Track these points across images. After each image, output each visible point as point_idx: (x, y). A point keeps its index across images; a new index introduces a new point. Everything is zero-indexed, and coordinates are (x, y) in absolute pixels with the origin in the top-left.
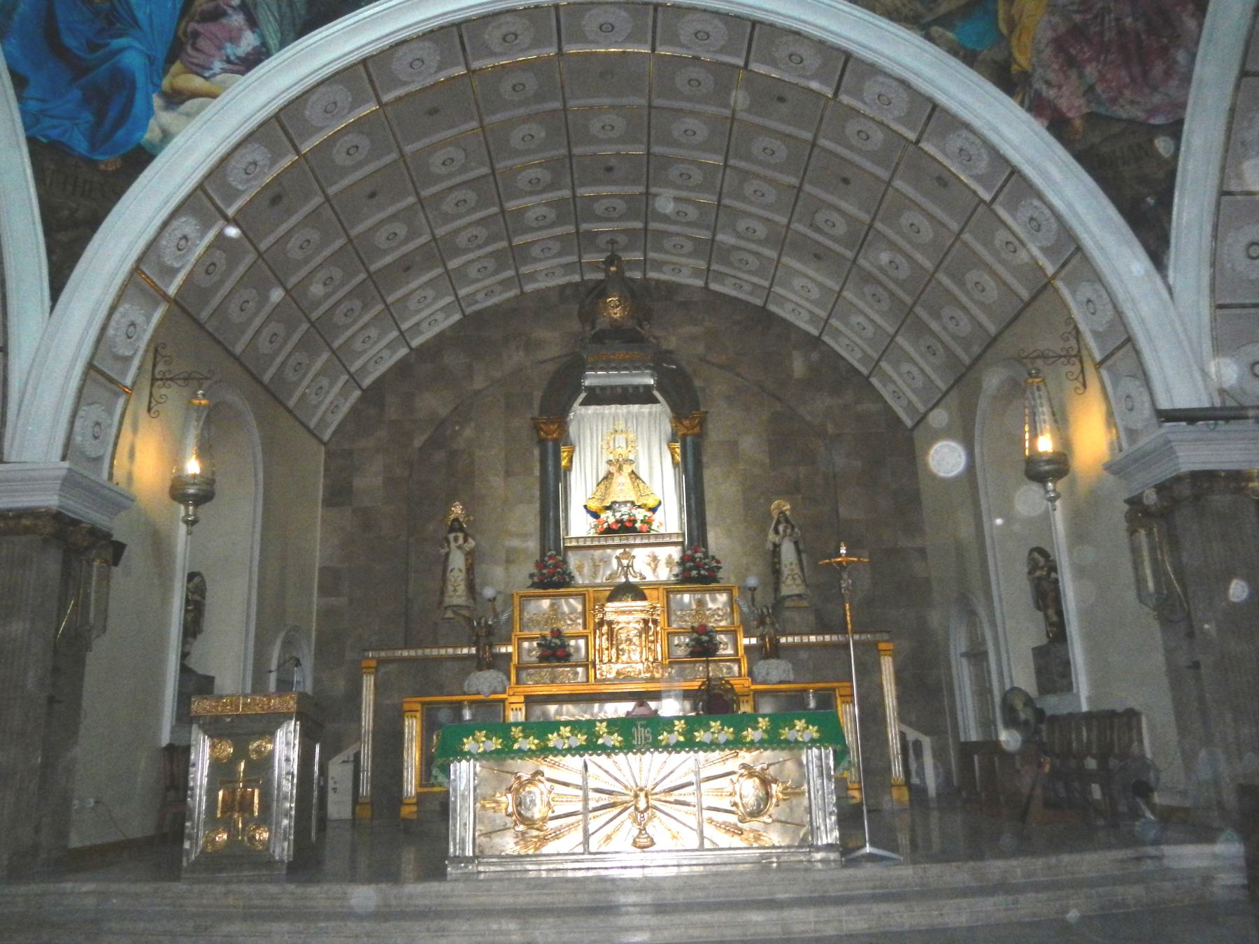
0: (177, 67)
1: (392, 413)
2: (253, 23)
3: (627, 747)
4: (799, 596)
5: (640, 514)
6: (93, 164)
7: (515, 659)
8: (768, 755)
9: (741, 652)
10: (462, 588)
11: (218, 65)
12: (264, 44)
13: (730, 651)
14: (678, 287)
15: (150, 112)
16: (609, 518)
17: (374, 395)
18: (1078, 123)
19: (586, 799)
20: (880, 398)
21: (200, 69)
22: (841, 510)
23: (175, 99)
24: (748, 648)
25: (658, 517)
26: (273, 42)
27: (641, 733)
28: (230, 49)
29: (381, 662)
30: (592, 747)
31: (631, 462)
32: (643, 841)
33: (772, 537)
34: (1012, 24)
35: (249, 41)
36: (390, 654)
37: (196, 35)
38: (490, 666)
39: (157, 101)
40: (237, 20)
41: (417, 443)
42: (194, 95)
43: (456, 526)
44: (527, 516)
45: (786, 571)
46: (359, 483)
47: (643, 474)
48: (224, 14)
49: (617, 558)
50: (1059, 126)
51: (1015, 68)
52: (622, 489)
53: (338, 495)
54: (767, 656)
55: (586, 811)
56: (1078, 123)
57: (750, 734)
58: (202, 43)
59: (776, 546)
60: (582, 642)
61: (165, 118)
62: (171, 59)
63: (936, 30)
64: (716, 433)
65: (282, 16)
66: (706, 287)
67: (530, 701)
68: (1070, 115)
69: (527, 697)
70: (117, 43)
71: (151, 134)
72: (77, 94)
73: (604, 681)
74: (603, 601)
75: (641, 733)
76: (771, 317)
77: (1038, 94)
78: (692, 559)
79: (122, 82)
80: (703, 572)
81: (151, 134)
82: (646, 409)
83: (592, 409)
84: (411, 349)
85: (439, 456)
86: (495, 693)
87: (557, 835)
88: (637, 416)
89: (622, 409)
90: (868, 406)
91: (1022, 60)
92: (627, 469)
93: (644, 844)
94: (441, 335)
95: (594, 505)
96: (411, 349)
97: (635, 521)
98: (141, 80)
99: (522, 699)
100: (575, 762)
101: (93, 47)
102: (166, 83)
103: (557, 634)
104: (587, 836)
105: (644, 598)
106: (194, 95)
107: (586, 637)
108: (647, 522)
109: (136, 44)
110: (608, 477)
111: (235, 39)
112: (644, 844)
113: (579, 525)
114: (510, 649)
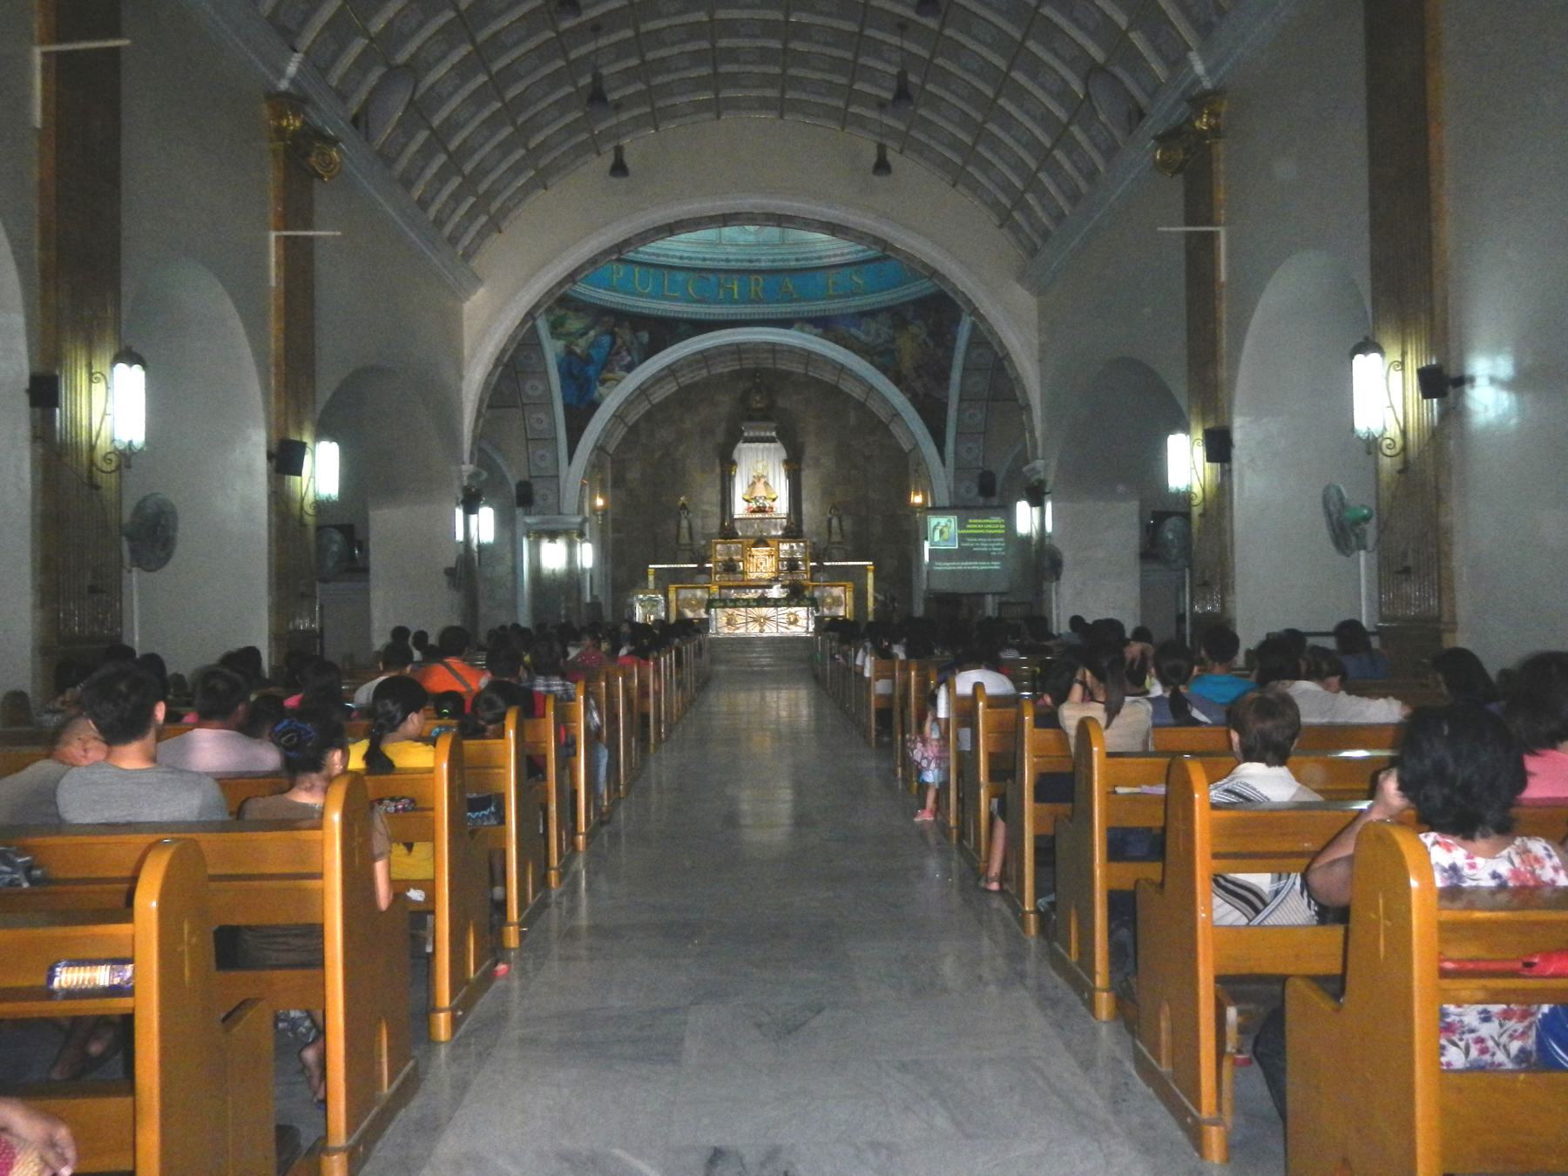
0: (604, 371)
2: (629, 353)
3: (758, 606)
4: (839, 543)
5: (768, 503)
8: (797, 609)
10: (687, 536)
11: (617, 369)
12: (633, 360)
13: (803, 568)
14: (792, 373)
15: (596, 387)
16: (753, 505)
17: (633, 430)
20: (891, 436)
21: (612, 371)
23: (603, 382)
25: (776, 504)
26: (636, 360)
27: (762, 602)
29: (656, 569)
30: (748, 606)
31: (763, 476)
33: (829, 516)
35: (629, 358)
39: (598, 384)
40: (624, 353)
41: (658, 454)
42: (610, 379)
43: (684, 506)
44: (712, 495)
45: (833, 531)
46: (630, 476)
47: (771, 483)
50: (915, 401)
52: (760, 491)
53: (618, 482)
57: (792, 603)
59: (830, 521)
61: (601, 389)
62: (603, 369)
63: (875, 358)
64: (810, 451)
66: (806, 375)
67: (721, 588)
71: (596, 395)
73: (751, 580)
75: (762, 602)
76: (841, 392)
82: (773, 445)
83: (746, 445)
87: (738, 628)
88: (769, 450)
89: (761, 445)
92: (763, 480)
93: (762, 631)
95: (747, 497)
100: (743, 609)
102: (601, 377)
103: (731, 560)
105: (768, 546)
106: (610, 379)
108: (771, 508)
110: (754, 483)
111: (623, 360)
112: (762, 631)
113: (740, 509)
114: (711, 565)
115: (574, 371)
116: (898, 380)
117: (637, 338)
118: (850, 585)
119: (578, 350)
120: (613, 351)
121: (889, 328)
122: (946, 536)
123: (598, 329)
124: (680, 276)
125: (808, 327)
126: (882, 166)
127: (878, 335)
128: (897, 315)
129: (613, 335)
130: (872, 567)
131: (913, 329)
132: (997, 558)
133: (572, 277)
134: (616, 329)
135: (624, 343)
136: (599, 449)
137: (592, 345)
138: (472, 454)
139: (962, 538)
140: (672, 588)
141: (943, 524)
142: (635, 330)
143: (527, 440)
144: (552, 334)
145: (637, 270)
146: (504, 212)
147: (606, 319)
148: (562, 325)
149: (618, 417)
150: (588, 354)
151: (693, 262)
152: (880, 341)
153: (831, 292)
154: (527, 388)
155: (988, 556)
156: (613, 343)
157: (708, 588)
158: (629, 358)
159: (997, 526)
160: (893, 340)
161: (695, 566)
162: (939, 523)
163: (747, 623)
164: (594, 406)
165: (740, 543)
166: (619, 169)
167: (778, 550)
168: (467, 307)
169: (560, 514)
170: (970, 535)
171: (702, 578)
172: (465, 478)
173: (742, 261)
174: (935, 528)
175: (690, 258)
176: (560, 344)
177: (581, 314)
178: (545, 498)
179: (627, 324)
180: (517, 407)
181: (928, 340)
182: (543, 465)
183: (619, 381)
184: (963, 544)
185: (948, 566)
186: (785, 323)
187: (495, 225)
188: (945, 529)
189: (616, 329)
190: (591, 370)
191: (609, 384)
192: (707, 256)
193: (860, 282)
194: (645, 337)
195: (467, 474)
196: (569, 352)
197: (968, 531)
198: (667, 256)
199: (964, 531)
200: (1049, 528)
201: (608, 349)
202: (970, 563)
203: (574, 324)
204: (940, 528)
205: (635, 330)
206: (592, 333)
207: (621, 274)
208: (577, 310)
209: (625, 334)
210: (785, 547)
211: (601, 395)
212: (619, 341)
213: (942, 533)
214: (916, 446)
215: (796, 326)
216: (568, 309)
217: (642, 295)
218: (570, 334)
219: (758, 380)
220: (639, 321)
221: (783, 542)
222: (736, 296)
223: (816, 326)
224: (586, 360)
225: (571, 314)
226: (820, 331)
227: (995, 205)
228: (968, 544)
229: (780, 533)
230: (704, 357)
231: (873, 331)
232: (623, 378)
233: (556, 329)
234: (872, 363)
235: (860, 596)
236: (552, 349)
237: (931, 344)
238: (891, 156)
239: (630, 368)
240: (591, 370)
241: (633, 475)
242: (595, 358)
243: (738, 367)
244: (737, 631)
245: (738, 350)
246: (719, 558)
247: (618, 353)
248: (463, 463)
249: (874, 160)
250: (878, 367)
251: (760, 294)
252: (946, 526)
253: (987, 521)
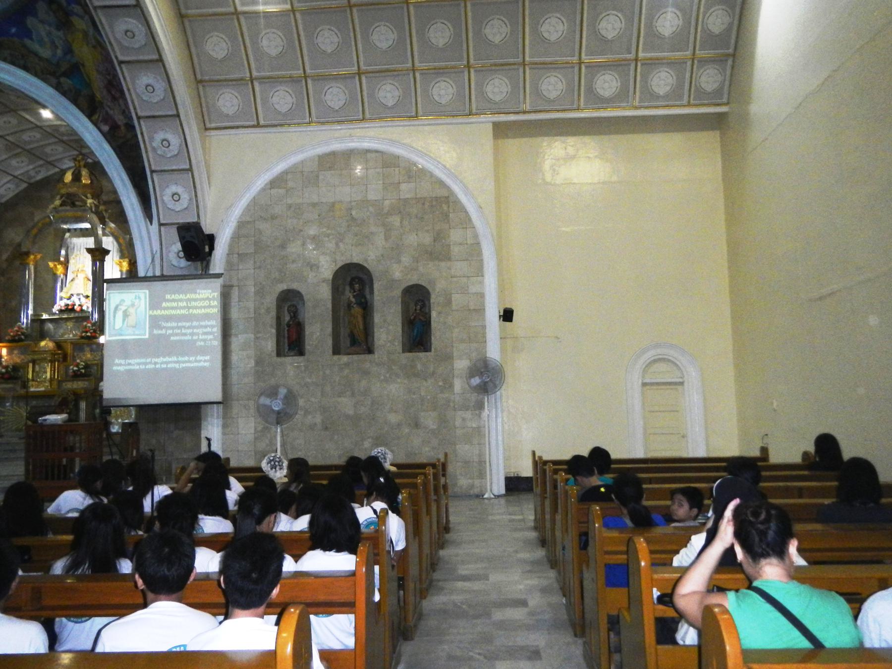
18: (123, 128)
56: (123, 128)
63: (62, 80)
68: (119, 123)
77: (107, 113)
78: (86, 327)
80: (89, 334)
94: (17, 195)
97: (74, 305)
122: (131, 320)
132: (203, 351)
139: (155, 322)
141: (128, 303)
155: (186, 348)
159: (206, 303)
162: (123, 301)
170: (169, 318)
174: (116, 308)
184: (155, 332)
185: (136, 364)
188: (132, 310)
197: (163, 312)
199: (158, 312)
202: (167, 359)
204: (123, 308)
213: (126, 315)
228: (163, 332)
250: (64, 94)
252: (133, 305)
253: (193, 296)
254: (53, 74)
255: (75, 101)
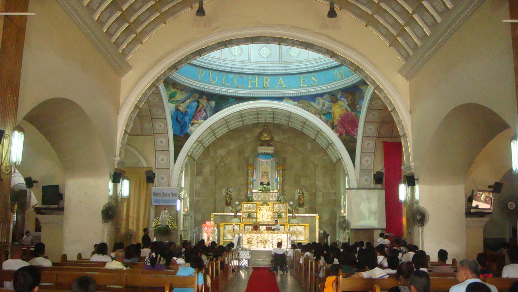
0: (193, 119)
1: (212, 154)
2: (205, 111)
6: (180, 136)
7: (242, 216)
9: (288, 217)
11: (199, 119)
14: (282, 125)
15: (189, 127)
17: (207, 149)
19: (257, 241)
20: (328, 155)
21: (197, 120)
22: (317, 182)
23: (193, 124)
24: (289, 216)
26: (208, 114)
28: (201, 116)
29: (215, 215)
32: (265, 247)
34: (334, 117)
35: (205, 114)
36: (216, 214)
37: (197, 114)
38: (236, 217)
39: (190, 125)
40: (203, 111)
41: (218, 161)
42: (195, 123)
48: (201, 111)
49: (264, 195)
51: (335, 124)
54: (293, 218)
55: (257, 243)
58: (197, 116)
60: (255, 214)
62: (192, 119)
63: (322, 116)
65: (210, 110)
67: (245, 225)
69: (245, 224)
70: (185, 118)
71: (189, 131)
72: (179, 127)
74: (260, 205)
79: (186, 124)
81: (189, 131)
84: (216, 138)
85: (223, 164)
86: (237, 223)
87: (253, 245)
90: (325, 158)
91: (336, 123)
93: (264, 247)
96: (216, 138)
98: (188, 123)
99: (244, 225)
101: (182, 119)
104: (257, 246)
107: (256, 213)
109: (188, 117)
112: (264, 247)
115: (179, 119)
116: (333, 127)
117: (209, 104)
118: (307, 225)
119: (181, 109)
120: (198, 110)
121: (329, 102)
123: (191, 99)
124: (231, 76)
125: (291, 102)
126: (332, 14)
127: (324, 105)
128: (333, 96)
129: (198, 102)
130: (318, 217)
131: (340, 102)
133: (175, 67)
134: (199, 100)
135: (203, 106)
136: (190, 156)
137: (188, 107)
138: (120, 152)
140: (222, 225)
142: (208, 100)
143: (155, 151)
144: (169, 101)
145: (210, 73)
146: (145, 32)
147: (195, 95)
148: (174, 97)
149: (199, 141)
150: (186, 111)
151: (237, 70)
152: (324, 108)
153: (301, 85)
154: (156, 125)
156: (198, 107)
157: (239, 225)
158: (205, 114)
160: (331, 109)
161: (233, 214)
163: (257, 243)
164: (187, 136)
165: (256, 204)
166: (201, 12)
167: (273, 208)
168: (123, 79)
169: (169, 187)
171: (236, 220)
172: (116, 164)
173: (260, 70)
175: (236, 68)
176: (173, 106)
177: (183, 91)
178: (163, 178)
179: (205, 97)
180: (152, 135)
181: (348, 108)
182: (162, 163)
183: (200, 124)
186: (280, 99)
187: (138, 40)
189: (199, 100)
190: (187, 119)
191: (195, 125)
192: (244, 67)
193: (316, 80)
194: (213, 103)
195: (117, 162)
196: (177, 110)
198: (225, 67)
200: (417, 197)
201: (195, 109)
203: (180, 96)
205: (208, 100)
206: (188, 101)
207: (203, 74)
208: (182, 90)
209: (204, 102)
210: (277, 206)
211: (191, 130)
212: (201, 106)
214: (339, 160)
215: (284, 100)
216: (178, 89)
217: (213, 84)
218: (178, 101)
219: (266, 128)
220: (210, 96)
221: (276, 204)
222: (257, 86)
223: (294, 101)
224: (185, 114)
225: (178, 92)
226: (296, 103)
227: (387, 35)
229: (275, 199)
230: (241, 115)
231: (321, 104)
232: (202, 123)
233: (171, 97)
234: (320, 118)
235: (312, 231)
236: (169, 108)
237: (349, 109)
238: (337, 8)
239: (205, 118)
240: (187, 119)
241: (207, 170)
242: (189, 114)
243: (256, 122)
244: (252, 247)
245: (257, 112)
246: (245, 210)
247: (200, 111)
248: (116, 156)
249: (327, 9)
251: (268, 85)
254: (319, 114)
255: (327, 124)
